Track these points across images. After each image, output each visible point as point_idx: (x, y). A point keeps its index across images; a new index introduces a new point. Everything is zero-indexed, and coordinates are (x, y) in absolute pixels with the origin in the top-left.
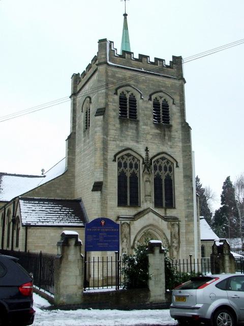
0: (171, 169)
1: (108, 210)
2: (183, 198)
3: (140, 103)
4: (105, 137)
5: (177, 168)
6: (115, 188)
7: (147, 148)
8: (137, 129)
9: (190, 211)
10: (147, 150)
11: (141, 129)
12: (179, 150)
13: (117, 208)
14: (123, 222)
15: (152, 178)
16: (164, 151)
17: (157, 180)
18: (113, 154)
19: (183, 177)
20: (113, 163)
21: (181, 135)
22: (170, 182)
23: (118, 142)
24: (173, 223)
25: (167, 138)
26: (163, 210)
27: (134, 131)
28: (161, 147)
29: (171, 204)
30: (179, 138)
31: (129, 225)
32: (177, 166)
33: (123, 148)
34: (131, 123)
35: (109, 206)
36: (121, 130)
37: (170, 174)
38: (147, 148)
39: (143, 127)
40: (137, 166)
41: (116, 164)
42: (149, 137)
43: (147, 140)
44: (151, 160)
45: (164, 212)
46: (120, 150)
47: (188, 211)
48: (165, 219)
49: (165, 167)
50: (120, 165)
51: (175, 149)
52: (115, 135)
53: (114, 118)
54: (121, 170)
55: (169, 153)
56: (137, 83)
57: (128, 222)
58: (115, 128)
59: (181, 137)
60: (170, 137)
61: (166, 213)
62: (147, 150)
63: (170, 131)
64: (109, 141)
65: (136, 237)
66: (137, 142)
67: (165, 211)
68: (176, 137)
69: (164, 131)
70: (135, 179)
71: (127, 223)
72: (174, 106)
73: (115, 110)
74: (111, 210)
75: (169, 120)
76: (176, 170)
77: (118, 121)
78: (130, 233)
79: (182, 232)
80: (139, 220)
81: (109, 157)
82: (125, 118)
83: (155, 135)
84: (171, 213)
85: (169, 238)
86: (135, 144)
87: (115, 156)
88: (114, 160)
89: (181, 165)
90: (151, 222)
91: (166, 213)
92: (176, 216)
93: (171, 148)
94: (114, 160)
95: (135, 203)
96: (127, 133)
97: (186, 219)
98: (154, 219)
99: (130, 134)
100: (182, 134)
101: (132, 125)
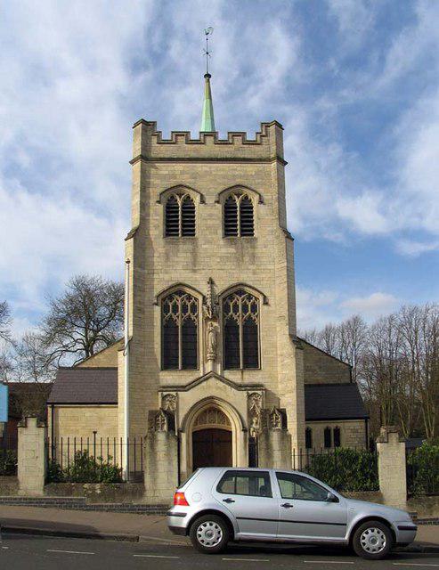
0: (254, 308)
3: (200, 210)
4: (139, 270)
5: (265, 307)
7: (211, 279)
8: (194, 254)
10: (211, 282)
11: (201, 251)
14: (165, 393)
17: (230, 328)
22: (252, 330)
24: (250, 392)
25: (247, 259)
27: (189, 255)
29: (252, 361)
32: (266, 303)
33: (171, 283)
34: (184, 243)
37: (253, 317)
38: (211, 279)
39: (203, 247)
40: (194, 308)
45: (240, 377)
48: (239, 387)
50: (165, 309)
56: (195, 178)
57: (174, 393)
60: (253, 256)
62: (211, 282)
63: (254, 247)
65: (187, 416)
66: (194, 271)
70: (190, 329)
82: (176, 237)
83: (225, 259)
84: (251, 377)
85: (245, 418)
86: (190, 275)
90: (214, 393)
95: (191, 363)
96: (176, 259)
98: (218, 388)
101: (184, 246)
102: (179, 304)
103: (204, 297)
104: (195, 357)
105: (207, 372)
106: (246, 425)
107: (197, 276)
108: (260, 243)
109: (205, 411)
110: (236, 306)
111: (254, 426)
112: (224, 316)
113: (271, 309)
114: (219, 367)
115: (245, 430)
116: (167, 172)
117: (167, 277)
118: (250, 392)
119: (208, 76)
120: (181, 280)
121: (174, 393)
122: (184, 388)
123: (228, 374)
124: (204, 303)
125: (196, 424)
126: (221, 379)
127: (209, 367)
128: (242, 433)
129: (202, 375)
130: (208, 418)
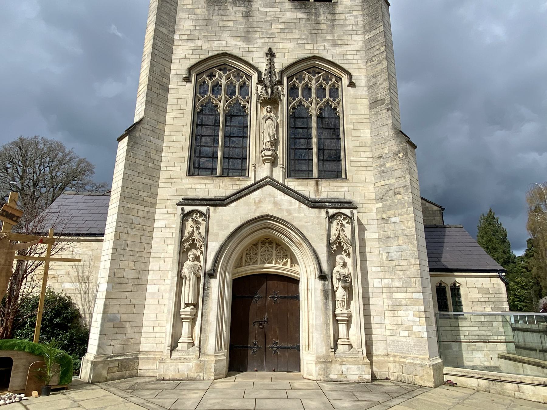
0: (334, 91)
2: (369, 154)
5: (351, 90)
6: (185, 135)
7: (270, 50)
8: (247, 14)
9: (387, 182)
10: (271, 54)
13: (185, 181)
14: (188, 209)
16: (316, 53)
18: (187, 66)
19: (367, 107)
20: (184, 83)
21: (360, 18)
23: (199, 43)
24: (332, 212)
26: (312, 183)
28: (308, 47)
30: (356, 25)
32: (352, 85)
33: (211, 54)
35: (163, 175)
36: (208, 23)
38: (270, 50)
40: (245, 89)
41: (190, 86)
42: (276, 28)
43: (273, 33)
44: (282, 72)
46: (202, 57)
47: (382, 183)
50: (200, 89)
52: (192, 28)
54: (202, 99)
55: (329, 57)
58: (193, 16)
59: (360, 23)
60: (332, 24)
61: (317, 191)
62: (271, 54)
64: (176, 43)
66: (247, 39)
67: (317, 185)
68: (348, 22)
69: (317, 14)
71: (200, 212)
76: (346, 92)
79: (371, 240)
81: (173, 72)
86: (241, 44)
88: (187, 79)
89: (361, 80)
90: (267, 209)
91: (317, 191)
92: (348, 197)
93: (334, 44)
94: (187, 79)
97: (380, 205)
99: (231, 24)
102: (223, 82)
103: (260, 73)
104: (244, 158)
105: (258, 179)
107: (252, 47)
108: (340, 8)
109: (256, 245)
110: (307, 89)
111: (337, 268)
112: (289, 103)
113: (359, 92)
114: (278, 174)
115: (323, 277)
117: (206, 46)
118: (332, 212)
120: (228, 50)
121: (203, 209)
123: (291, 184)
124: (260, 81)
125: (239, 264)
127: (263, 171)
128: (320, 283)
130: (259, 256)
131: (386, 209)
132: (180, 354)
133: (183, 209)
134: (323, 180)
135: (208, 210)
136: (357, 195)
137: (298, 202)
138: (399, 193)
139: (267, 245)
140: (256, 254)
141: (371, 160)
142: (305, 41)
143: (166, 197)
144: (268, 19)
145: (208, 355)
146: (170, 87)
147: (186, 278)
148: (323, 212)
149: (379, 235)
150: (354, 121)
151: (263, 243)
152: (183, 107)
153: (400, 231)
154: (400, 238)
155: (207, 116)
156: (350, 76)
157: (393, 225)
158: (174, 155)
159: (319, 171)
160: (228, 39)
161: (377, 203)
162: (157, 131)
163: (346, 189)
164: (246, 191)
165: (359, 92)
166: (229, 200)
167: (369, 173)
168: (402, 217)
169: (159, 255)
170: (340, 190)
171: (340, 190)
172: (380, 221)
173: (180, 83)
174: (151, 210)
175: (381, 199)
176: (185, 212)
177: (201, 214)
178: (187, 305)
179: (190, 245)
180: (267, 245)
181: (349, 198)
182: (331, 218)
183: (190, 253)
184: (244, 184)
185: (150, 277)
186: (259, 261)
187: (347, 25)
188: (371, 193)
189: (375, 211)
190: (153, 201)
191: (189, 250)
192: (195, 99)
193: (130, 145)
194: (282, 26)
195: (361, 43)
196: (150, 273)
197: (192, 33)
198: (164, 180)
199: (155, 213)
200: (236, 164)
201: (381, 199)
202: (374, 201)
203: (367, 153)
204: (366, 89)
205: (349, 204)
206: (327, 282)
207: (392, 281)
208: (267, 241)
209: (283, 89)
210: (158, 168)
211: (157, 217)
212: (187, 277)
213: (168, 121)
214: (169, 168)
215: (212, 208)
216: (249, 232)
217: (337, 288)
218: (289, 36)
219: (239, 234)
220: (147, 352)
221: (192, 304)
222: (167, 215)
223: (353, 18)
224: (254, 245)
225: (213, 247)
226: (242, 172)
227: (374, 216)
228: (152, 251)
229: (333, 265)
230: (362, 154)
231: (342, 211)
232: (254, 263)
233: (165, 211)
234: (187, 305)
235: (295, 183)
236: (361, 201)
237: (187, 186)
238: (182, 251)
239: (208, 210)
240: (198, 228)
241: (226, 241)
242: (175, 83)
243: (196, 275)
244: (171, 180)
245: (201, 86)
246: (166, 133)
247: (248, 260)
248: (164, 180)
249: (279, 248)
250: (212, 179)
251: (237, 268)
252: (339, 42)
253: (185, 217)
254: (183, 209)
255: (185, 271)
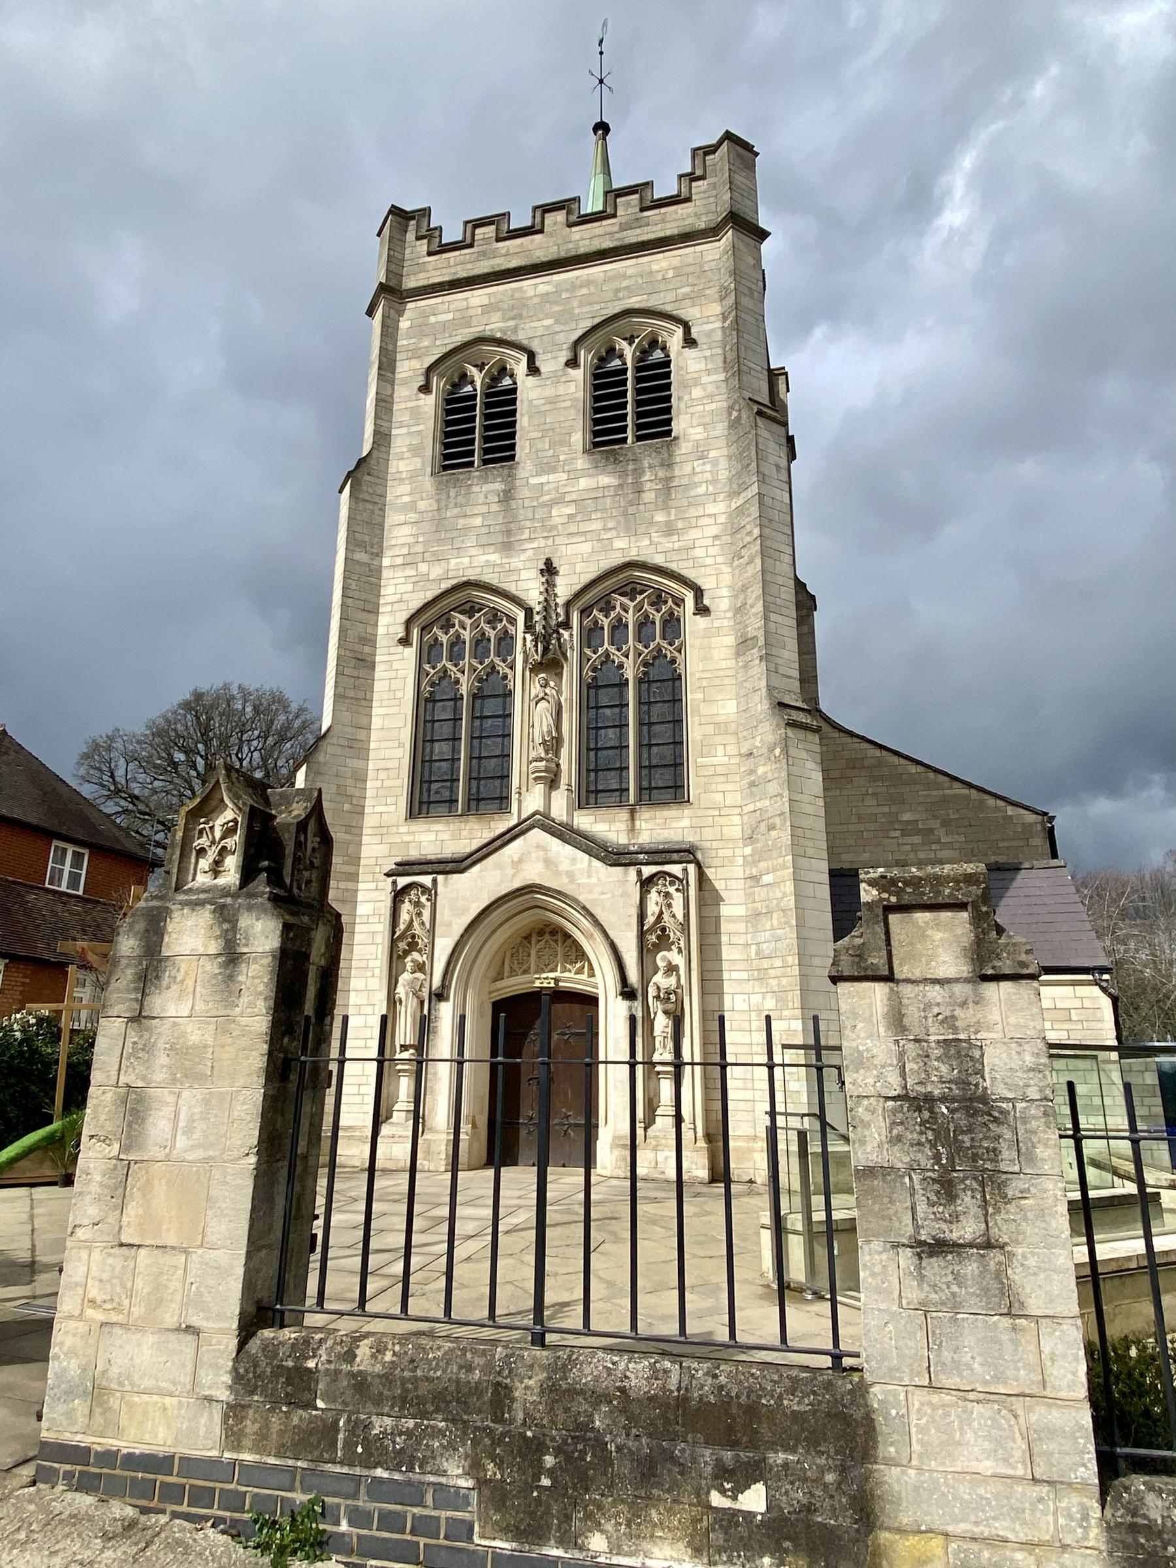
0: (673, 625)
1: (365, 839)
2: (732, 750)
3: (529, 391)
5: (702, 622)
8: (507, 496)
9: (759, 805)
10: (549, 570)
11: (525, 493)
12: (715, 530)
14: (402, 881)
15: (569, 685)
16: (633, 555)
18: (405, 616)
21: (723, 464)
23: (423, 568)
24: (648, 871)
26: (624, 815)
28: (619, 544)
30: (714, 481)
31: (431, 892)
32: (702, 610)
33: (445, 585)
35: (369, 821)
37: (669, 651)
40: (506, 642)
41: (411, 653)
42: (560, 513)
43: (554, 527)
44: (568, 604)
46: (430, 595)
47: (751, 807)
48: (616, 857)
49: (644, 624)
50: (428, 653)
51: (694, 534)
52: (411, 540)
53: (414, 475)
55: (659, 560)
58: (413, 517)
59: (723, 475)
60: (667, 488)
61: (632, 830)
62: (549, 570)
64: (386, 574)
66: (507, 547)
67: (633, 819)
69: (639, 472)
71: (422, 886)
72: (690, 353)
73: (415, 450)
74: (377, 839)
75: (668, 422)
76: (693, 625)
77: (428, 483)
78: (432, 932)
79: (731, 919)
80: (477, 868)
81: (381, 630)
86: (494, 558)
87: (409, 623)
88: (405, 641)
89: (720, 598)
90: (533, 873)
91: (632, 830)
92: (691, 838)
93: (670, 530)
94: (405, 641)
97: (748, 851)
99: (478, 521)
100: (729, 457)
103: (529, 612)
104: (505, 777)
105: (524, 816)
106: (633, 976)
107: (517, 562)
108: (683, 449)
109: (527, 938)
111: (659, 978)
113: (717, 624)
114: (560, 806)
115: (628, 993)
116: (450, 316)
117: (436, 571)
118: (648, 871)
119: (602, 128)
120: (472, 575)
121: (426, 880)
122: (458, 865)
123: (585, 821)
124: (529, 627)
126: (566, 833)
129: (514, 821)
131: (757, 857)
132: (394, 1129)
133: (394, 883)
134: (644, 808)
135: (435, 881)
136: (708, 833)
137: (587, 856)
138: (774, 828)
139: (547, 936)
140: (529, 956)
141: (736, 760)
142: (613, 533)
143: (373, 861)
144: (546, 498)
145: (437, 1132)
146: (378, 659)
147: (401, 1002)
148: (632, 871)
149: (747, 910)
150: (705, 684)
151: (541, 933)
152: (399, 694)
153: (775, 902)
154: (775, 915)
155: (440, 704)
156: (699, 593)
157: (765, 889)
158: (386, 783)
159: (640, 789)
160: (474, 551)
161: (745, 846)
162: (355, 744)
163: (686, 823)
164: (499, 843)
165: (717, 624)
166: (469, 861)
167: (731, 787)
168: (778, 873)
169: (364, 964)
170: (674, 825)
171: (674, 825)
172: (749, 883)
173: (392, 650)
174: (350, 885)
175: (750, 839)
176: (399, 888)
177: (425, 889)
178: (404, 1048)
179: (409, 944)
180: (547, 936)
181: (691, 839)
182: (646, 884)
183: (408, 959)
184: (501, 825)
185: (351, 1002)
186: (533, 968)
187: (695, 485)
188: (734, 827)
189: (740, 861)
190: (352, 869)
191: (406, 953)
192: (420, 672)
193: (310, 778)
194: (570, 510)
195: (722, 519)
196: (352, 995)
197: (412, 551)
198: (369, 831)
199: (356, 891)
200: (490, 788)
201: (750, 839)
202: (741, 844)
203: (728, 748)
204: (729, 614)
205: (687, 853)
206: (636, 1003)
207: (764, 998)
208: (548, 930)
209: (571, 635)
210: (360, 809)
211: (360, 896)
212: (403, 999)
213: (376, 722)
214: (378, 809)
215: (440, 878)
216: (504, 918)
217: (655, 1013)
218: (584, 527)
219: (486, 922)
220: (350, 1127)
221: (411, 1046)
222: (376, 893)
223: (708, 467)
224: (526, 938)
225: (443, 946)
226: (502, 802)
227: (739, 872)
228: (354, 957)
229: (646, 974)
230: (720, 749)
231: (667, 868)
232: (526, 972)
233: (372, 885)
234: (404, 1048)
235: (592, 818)
236: (715, 845)
237: (407, 838)
238: (395, 957)
239: (435, 881)
240: (419, 914)
241: (462, 936)
242: (385, 651)
243: (418, 997)
244: (382, 830)
245: (431, 647)
246: (372, 745)
247: (515, 967)
248: (369, 831)
249: (569, 941)
250: (448, 822)
251: (495, 980)
252: (680, 525)
253: (398, 896)
254: (394, 883)
255: (401, 991)
